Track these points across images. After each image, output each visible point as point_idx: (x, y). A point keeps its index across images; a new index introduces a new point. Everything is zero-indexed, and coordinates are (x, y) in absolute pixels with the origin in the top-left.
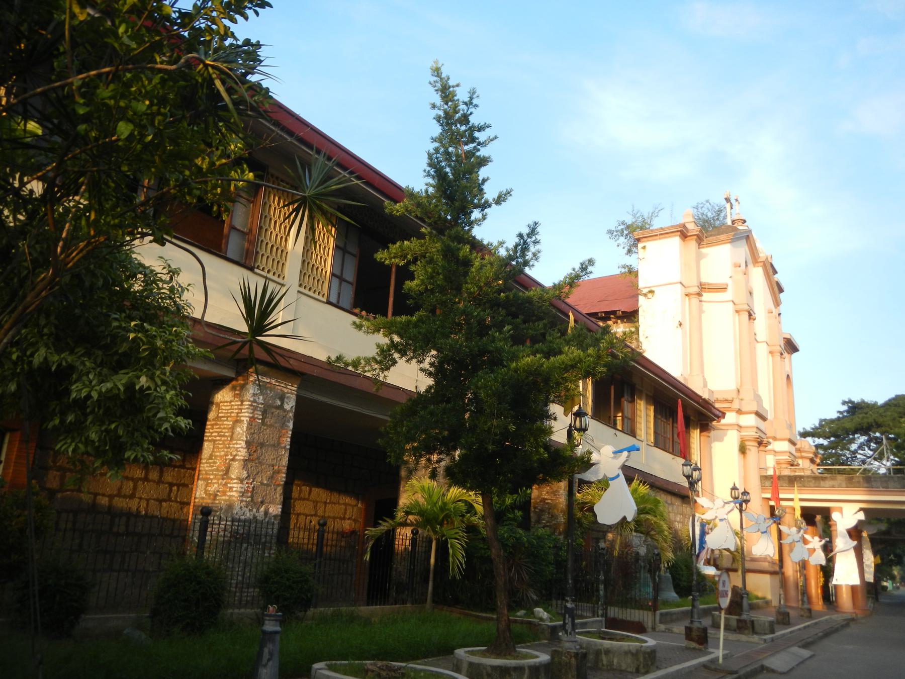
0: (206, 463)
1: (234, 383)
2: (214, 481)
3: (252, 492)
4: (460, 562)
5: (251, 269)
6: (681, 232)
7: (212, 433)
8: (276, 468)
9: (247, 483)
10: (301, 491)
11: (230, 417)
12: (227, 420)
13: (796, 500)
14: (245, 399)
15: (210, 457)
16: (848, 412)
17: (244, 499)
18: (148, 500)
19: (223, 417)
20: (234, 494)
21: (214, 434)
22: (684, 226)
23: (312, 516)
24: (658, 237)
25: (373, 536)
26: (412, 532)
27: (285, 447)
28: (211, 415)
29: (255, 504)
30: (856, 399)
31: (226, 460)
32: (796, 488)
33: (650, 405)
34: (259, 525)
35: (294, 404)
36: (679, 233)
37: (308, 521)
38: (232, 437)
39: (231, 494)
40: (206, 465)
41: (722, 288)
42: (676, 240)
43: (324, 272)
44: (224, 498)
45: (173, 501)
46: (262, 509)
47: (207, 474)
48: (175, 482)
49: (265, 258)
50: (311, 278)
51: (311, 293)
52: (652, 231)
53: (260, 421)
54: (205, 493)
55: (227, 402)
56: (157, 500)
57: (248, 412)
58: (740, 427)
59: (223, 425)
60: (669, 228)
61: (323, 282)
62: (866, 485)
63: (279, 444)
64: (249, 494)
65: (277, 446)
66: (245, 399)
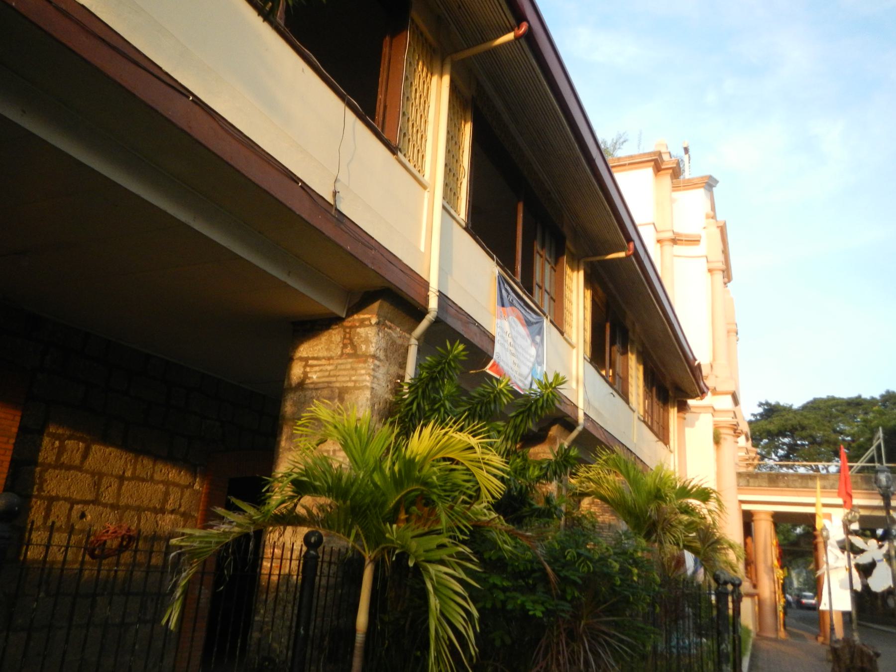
6: (656, 161)
10: (62, 450)
16: (761, 415)
22: (660, 154)
23: (86, 503)
24: (627, 167)
25: (193, 553)
30: (773, 402)
33: (640, 365)
36: (653, 163)
37: (75, 514)
41: (694, 241)
42: (649, 171)
52: (619, 159)
60: (641, 155)
62: (865, 486)
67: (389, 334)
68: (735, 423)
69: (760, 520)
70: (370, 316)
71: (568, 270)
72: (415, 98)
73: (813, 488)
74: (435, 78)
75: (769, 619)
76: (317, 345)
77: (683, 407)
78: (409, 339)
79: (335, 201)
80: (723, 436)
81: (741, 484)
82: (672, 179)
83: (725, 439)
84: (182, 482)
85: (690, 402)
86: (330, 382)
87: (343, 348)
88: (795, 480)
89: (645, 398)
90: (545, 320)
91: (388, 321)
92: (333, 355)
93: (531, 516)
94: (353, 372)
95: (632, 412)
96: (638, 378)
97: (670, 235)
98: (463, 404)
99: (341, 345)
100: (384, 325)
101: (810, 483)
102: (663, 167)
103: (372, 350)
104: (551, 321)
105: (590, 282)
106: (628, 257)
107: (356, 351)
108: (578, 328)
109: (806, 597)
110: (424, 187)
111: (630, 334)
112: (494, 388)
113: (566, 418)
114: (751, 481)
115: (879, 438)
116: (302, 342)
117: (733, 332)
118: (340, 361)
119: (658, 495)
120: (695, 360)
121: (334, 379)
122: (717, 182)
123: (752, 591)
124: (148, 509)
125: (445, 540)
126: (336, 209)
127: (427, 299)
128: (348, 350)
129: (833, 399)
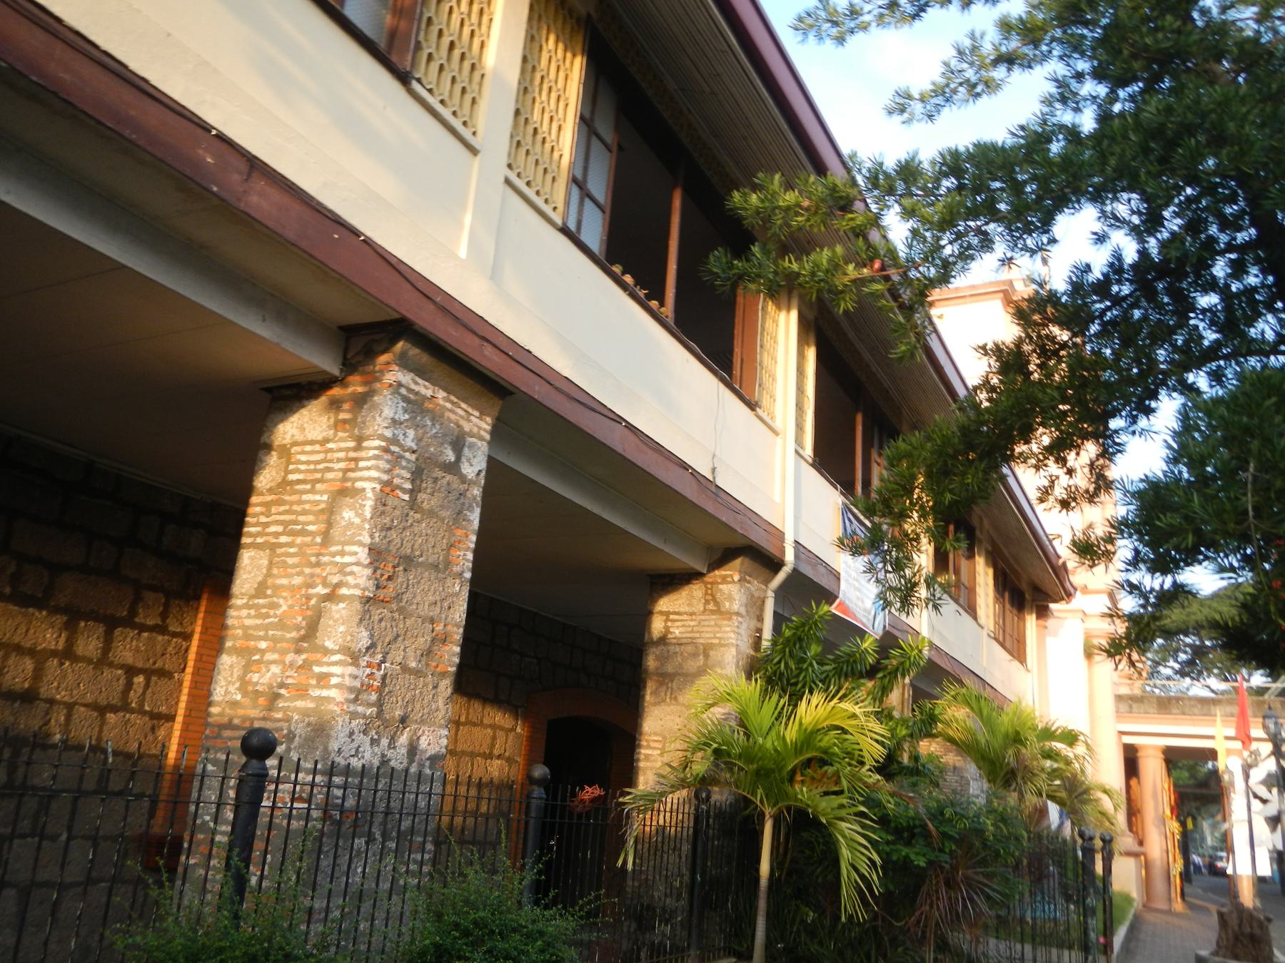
0: (247, 606)
1: (336, 391)
2: (269, 656)
3: (380, 690)
4: (862, 877)
5: (404, 78)
6: (1005, 292)
7: (267, 525)
8: (439, 628)
9: (369, 665)
11: (321, 481)
12: (312, 491)
13: (1220, 738)
14: (368, 432)
15: (260, 590)
17: (360, 709)
18: (70, 707)
19: (299, 482)
20: (333, 693)
21: (273, 529)
27: (461, 574)
28: (264, 480)
29: (386, 725)
31: (309, 598)
32: (1219, 719)
34: (398, 786)
35: (483, 465)
36: (1001, 295)
38: (326, 535)
39: (325, 693)
40: (244, 612)
43: (556, 155)
44: (300, 704)
45: (132, 711)
46: (403, 739)
47: (247, 637)
48: (140, 665)
49: (434, 67)
50: (531, 159)
51: (530, 193)
53: (406, 497)
54: (243, 689)
55: (312, 443)
56: (95, 706)
57: (377, 468)
59: (300, 502)
61: (554, 179)
63: (448, 563)
64: (374, 697)
65: (442, 568)
66: (368, 432)
67: (748, 589)
70: (733, 571)
75: (1159, 885)
76: (677, 599)
77: (1043, 612)
78: (765, 591)
84: (507, 726)
85: (1052, 606)
86: (694, 638)
87: (705, 604)
89: (996, 600)
93: (900, 773)
94: (717, 629)
96: (987, 584)
98: (827, 662)
103: (736, 607)
107: (719, 609)
110: (776, 433)
111: (978, 533)
112: (858, 646)
114: (1135, 706)
116: (661, 596)
118: (703, 617)
119: (1017, 739)
120: (1059, 557)
121: (698, 635)
123: (1136, 848)
124: (479, 755)
125: (845, 801)
126: (717, 486)
127: (783, 553)
128: (711, 606)
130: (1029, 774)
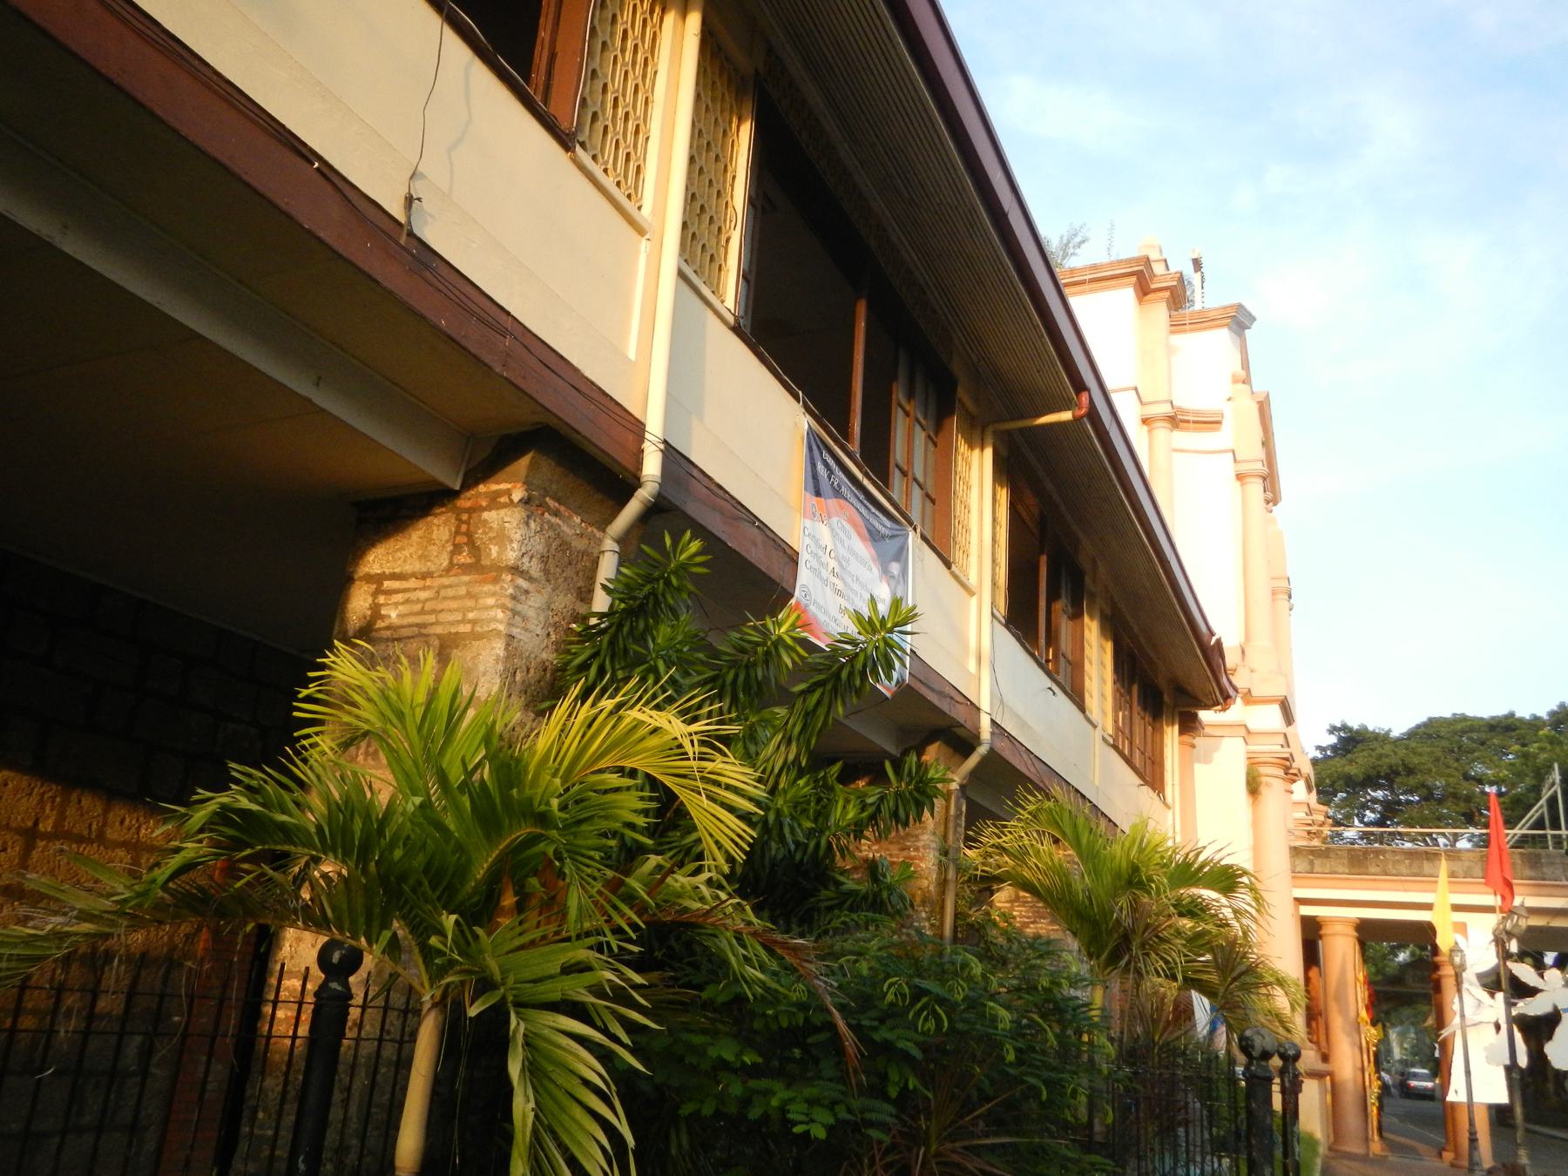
16: (1334, 748)
24: (1086, 287)
26: (323, 959)
30: (1354, 724)
33: (1107, 639)
36: (1134, 279)
41: (1211, 423)
42: (1126, 294)
52: (1072, 271)
58: (1248, 733)
60: (1111, 265)
62: (1528, 872)
67: (552, 526)
68: (1287, 755)
69: (1335, 934)
70: (511, 485)
71: (963, 447)
72: (623, 50)
73: (1431, 876)
74: (671, 18)
75: (1352, 1119)
76: (403, 549)
77: (1189, 724)
78: (600, 541)
79: (409, 218)
80: (1264, 779)
81: (1298, 869)
82: (1170, 309)
83: (1267, 784)
85: (1205, 715)
87: (453, 553)
88: (1398, 861)
90: (911, 534)
91: (553, 498)
92: (433, 568)
93: (840, 906)
94: (470, 603)
95: (1090, 727)
96: (1102, 664)
97: (1165, 409)
99: (450, 548)
100: (542, 505)
101: (1427, 867)
102: (1153, 286)
103: (511, 556)
104: (924, 538)
105: (1005, 470)
106: (1077, 420)
107: (478, 560)
108: (980, 557)
109: (1415, 1076)
110: (640, 231)
111: (1088, 580)
113: (955, 729)
114: (1317, 862)
115: (1553, 784)
116: (372, 544)
117: (1283, 593)
118: (446, 581)
119: (1133, 879)
120: (1212, 634)
121: (432, 618)
122: (1254, 319)
123: (1321, 1066)
125: (582, 953)
126: (411, 234)
128: (464, 558)
129: (1464, 718)
130: (1155, 940)
